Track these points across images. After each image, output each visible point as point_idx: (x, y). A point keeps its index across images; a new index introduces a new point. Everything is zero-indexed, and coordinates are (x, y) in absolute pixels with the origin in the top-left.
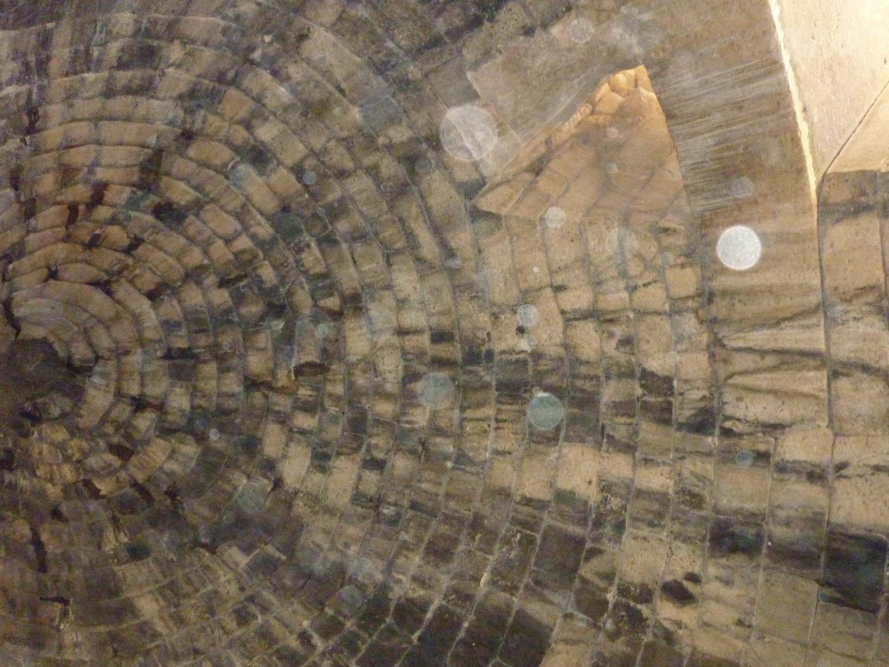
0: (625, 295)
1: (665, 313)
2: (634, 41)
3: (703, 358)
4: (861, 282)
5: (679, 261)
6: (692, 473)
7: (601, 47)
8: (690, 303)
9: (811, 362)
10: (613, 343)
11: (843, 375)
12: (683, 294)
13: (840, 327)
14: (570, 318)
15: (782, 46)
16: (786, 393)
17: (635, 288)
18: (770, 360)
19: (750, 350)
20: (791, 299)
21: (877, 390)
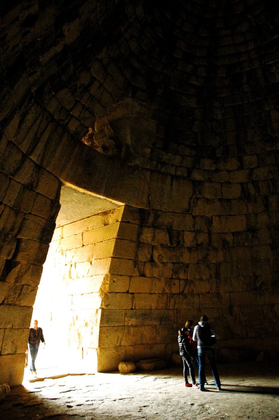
0: (83, 104)
1: (70, 111)
2: (132, 165)
3: (52, 110)
4: (40, 183)
5: (79, 129)
6: (36, 72)
7: (137, 156)
8: (67, 121)
9: (30, 150)
10: (78, 85)
11: (22, 159)
12: (71, 122)
13: (33, 168)
14: (93, 79)
15: (107, 198)
16: (28, 132)
17: (83, 109)
18: (39, 134)
19: (45, 130)
20: (49, 156)
21: (11, 168)
